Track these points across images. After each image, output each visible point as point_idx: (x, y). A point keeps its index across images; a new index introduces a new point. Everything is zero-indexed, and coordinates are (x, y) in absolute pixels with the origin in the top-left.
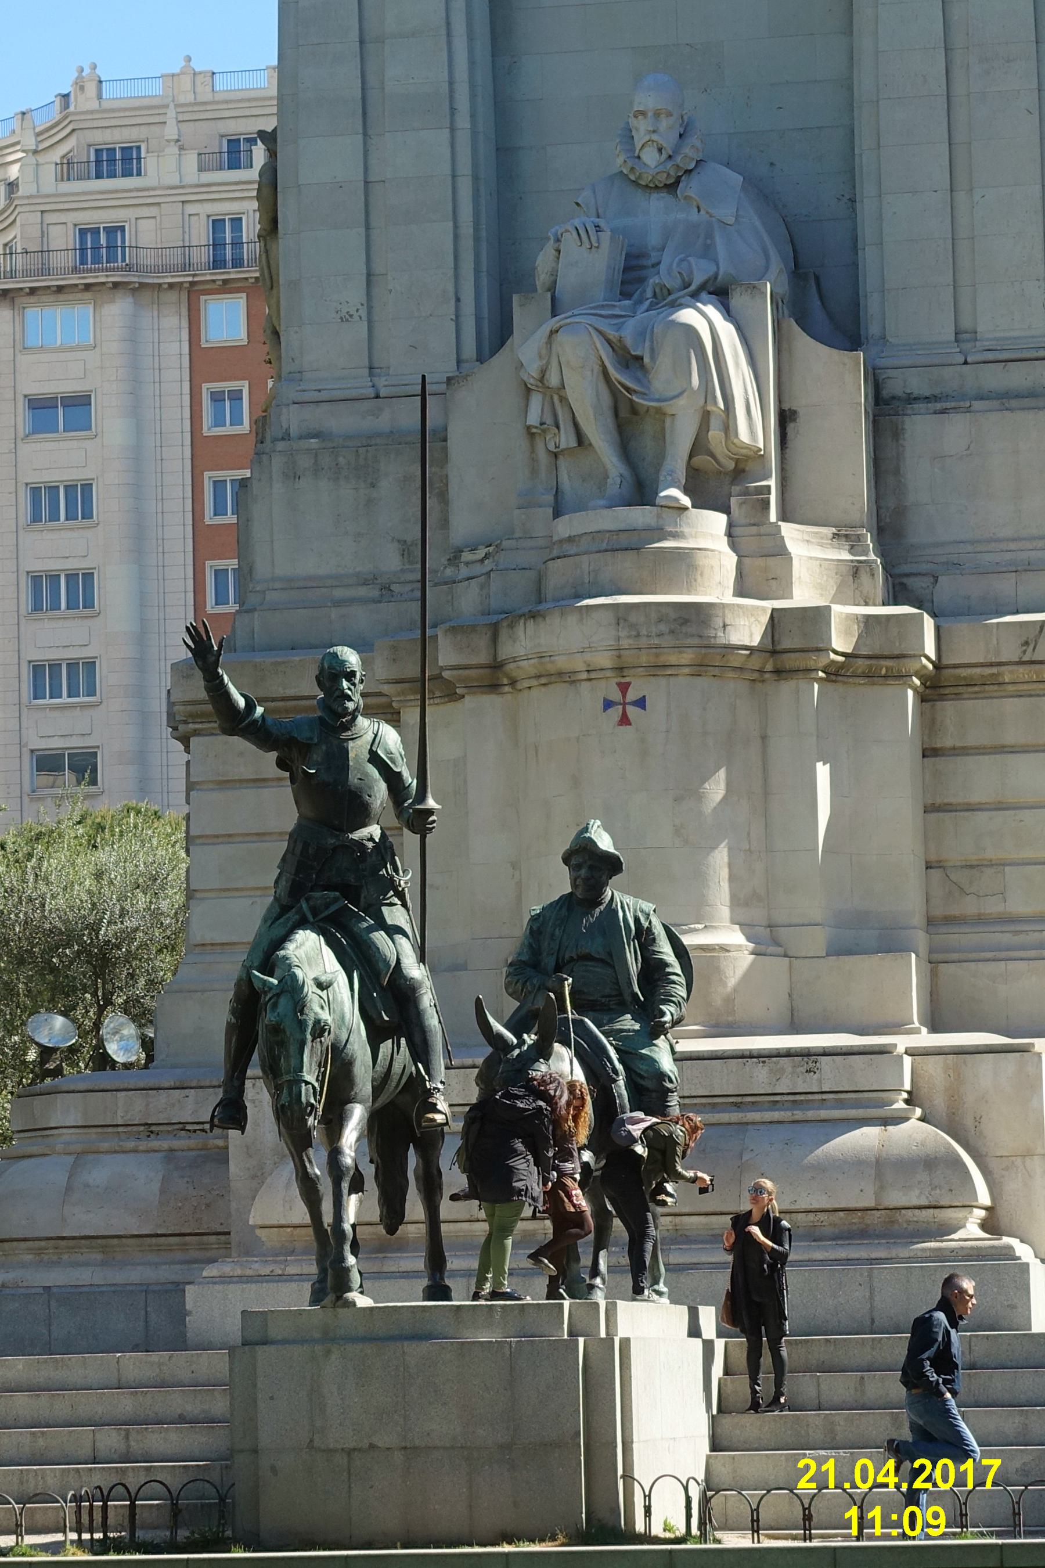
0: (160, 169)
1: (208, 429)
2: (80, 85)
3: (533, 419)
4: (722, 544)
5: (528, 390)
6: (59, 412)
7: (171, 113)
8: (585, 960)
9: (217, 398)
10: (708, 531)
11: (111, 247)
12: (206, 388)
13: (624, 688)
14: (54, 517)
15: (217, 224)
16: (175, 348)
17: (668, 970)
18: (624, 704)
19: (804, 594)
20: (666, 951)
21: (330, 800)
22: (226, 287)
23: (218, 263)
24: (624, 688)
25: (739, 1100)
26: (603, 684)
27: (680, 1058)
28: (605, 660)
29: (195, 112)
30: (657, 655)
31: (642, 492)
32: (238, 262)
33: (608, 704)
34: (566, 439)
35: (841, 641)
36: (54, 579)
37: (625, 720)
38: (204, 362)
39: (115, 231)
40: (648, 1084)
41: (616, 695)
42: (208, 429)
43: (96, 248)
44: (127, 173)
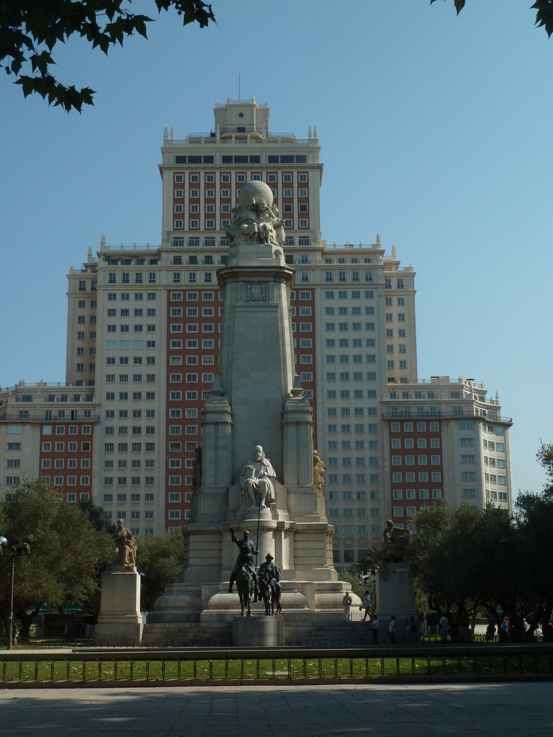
0: (38, 400)
1: (43, 451)
2: (20, 384)
3: (243, 493)
4: (270, 512)
5: (242, 490)
6: (15, 446)
7: (39, 390)
8: (269, 572)
9: (45, 445)
10: (268, 510)
11: (26, 416)
12: (43, 443)
14: (12, 466)
15: (47, 412)
16: (38, 435)
19: (280, 519)
21: (244, 550)
22: (48, 424)
23: (47, 419)
27: (281, 583)
29: (42, 391)
31: (259, 504)
32: (50, 419)
34: (247, 496)
35: (287, 526)
36: (11, 478)
38: (43, 438)
39: (27, 412)
42: (43, 451)
43: (23, 415)
44: (29, 401)
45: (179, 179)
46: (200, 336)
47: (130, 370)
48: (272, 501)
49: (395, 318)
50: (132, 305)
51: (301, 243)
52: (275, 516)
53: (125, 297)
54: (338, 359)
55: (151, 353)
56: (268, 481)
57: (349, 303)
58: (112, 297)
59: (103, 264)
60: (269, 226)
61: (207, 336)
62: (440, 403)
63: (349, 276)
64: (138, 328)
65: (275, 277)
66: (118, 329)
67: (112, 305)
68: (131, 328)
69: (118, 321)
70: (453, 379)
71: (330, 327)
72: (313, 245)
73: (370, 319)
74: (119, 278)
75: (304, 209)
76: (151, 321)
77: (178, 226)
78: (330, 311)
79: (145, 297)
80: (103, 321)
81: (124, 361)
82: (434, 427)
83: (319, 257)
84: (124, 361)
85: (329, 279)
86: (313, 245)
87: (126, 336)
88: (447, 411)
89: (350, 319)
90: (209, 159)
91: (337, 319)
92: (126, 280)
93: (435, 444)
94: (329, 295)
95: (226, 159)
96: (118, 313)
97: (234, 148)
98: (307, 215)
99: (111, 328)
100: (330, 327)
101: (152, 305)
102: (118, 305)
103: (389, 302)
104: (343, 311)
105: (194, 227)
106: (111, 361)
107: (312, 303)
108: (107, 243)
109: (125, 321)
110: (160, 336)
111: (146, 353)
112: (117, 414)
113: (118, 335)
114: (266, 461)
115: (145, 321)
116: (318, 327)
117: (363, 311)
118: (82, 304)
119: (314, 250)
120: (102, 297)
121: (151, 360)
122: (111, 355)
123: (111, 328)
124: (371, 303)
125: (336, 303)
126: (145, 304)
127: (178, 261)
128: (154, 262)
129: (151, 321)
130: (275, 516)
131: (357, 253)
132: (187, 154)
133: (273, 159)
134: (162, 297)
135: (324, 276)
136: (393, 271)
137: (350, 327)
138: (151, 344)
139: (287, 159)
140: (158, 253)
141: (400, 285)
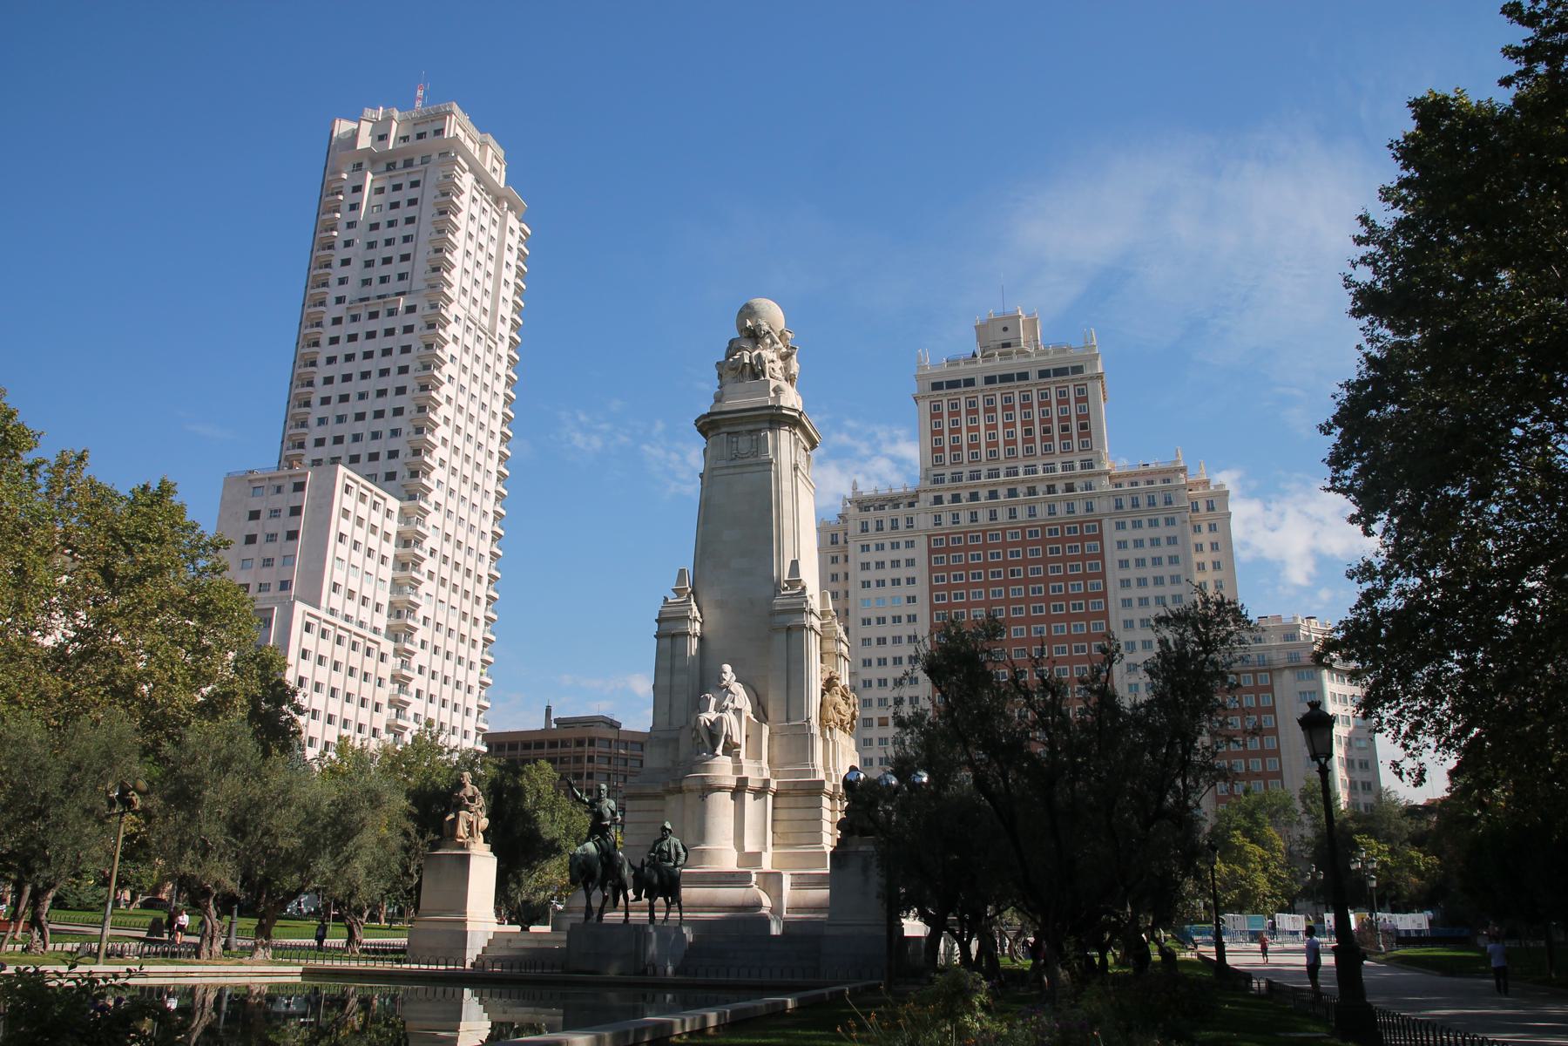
10: (727, 761)
45: (937, 408)
46: (968, 586)
47: (888, 631)
48: (738, 746)
49: (1207, 547)
50: (888, 555)
51: (1083, 467)
52: (738, 768)
53: (880, 547)
54: (1135, 603)
55: (912, 609)
56: (729, 717)
57: (1146, 533)
58: (865, 548)
59: (853, 511)
60: (768, 354)
61: (976, 585)
62: (1269, 648)
63: (1143, 501)
64: (896, 582)
65: (771, 422)
66: (873, 584)
67: (865, 557)
68: (888, 583)
69: (873, 575)
70: (1287, 618)
71: (1124, 564)
72: (1097, 468)
73: (1172, 550)
74: (872, 526)
75: (1084, 426)
76: (911, 572)
77: (938, 460)
78: (1122, 545)
79: (902, 545)
80: (858, 576)
81: (881, 620)
82: (1264, 679)
83: (1106, 481)
84: (881, 620)
85: (1119, 506)
86: (1097, 468)
87: (881, 591)
88: (1279, 658)
89: (1147, 552)
90: (970, 382)
91: (1131, 554)
92: (880, 527)
93: (1265, 700)
94: (1120, 526)
95: (990, 380)
96: (873, 565)
97: (998, 366)
98: (1089, 435)
99: (866, 584)
100: (1124, 564)
101: (910, 553)
102: (873, 557)
103: (1197, 529)
104: (1139, 543)
105: (956, 460)
106: (867, 622)
107: (1100, 537)
108: (860, 489)
109: (880, 574)
110: (921, 590)
111: (905, 610)
112: (875, 683)
113: (874, 591)
114: (737, 688)
115: (903, 573)
116: (1108, 565)
117: (1163, 541)
118: (834, 560)
119: (1100, 474)
120: (853, 548)
121: (912, 619)
122: (866, 616)
123: (866, 584)
124: (1171, 531)
125: (1129, 535)
126: (903, 554)
127: (938, 500)
128: (911, 505)
129: (911, 572)
130: (738, 768)
131: (1152, 473)
132: (944, 379)
133: (1044, 374)
134: (922, 544)
135: (1113, 503)
136: (1201, 491)
137: (1149, 562)
138: (911, 599)
139: (1060, 372)
140: (916, 495)
141: (1210, 507)
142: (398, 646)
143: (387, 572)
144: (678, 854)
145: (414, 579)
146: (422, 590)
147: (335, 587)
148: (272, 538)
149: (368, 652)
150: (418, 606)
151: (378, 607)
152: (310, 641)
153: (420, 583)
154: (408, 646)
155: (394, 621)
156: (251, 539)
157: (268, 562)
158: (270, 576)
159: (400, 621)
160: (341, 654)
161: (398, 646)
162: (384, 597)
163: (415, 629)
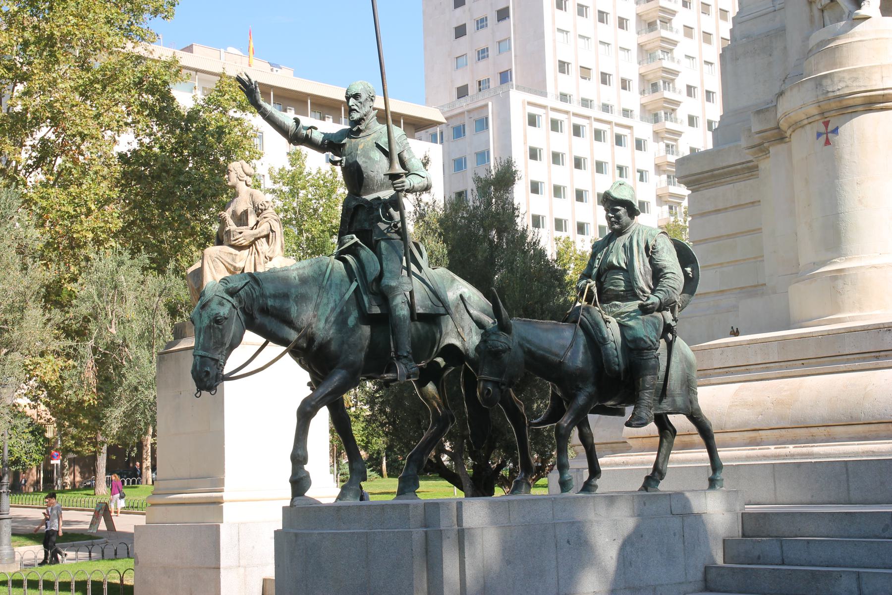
13: (826, 124)
17: (666, 271)
18: (827, 133)
20: (669, 259)
24: (826, 124)
25: (877, 354)
26: (815, 124)
28: (813, 110)
30: (840, 101)
33: (819, 135)
37: (827, 142)
40: (631, 346)
41: (822, 129)
142: (658, 127)
143: (631, 38)
144: (658, 274)
145: (664, 40)
146: (678, 52)
147: (563, 67)
148: (482, 23)
149: (619, 140)
150: (676, 73)
151: (625, 84)
152: (540, 137)
153: (674, 43)
154: (669, 125)
155: (648, 98)
156: (460, 31)
157: (483, 54)
158: (487, 70)
159: (657, 96)
160: (583, 147)
161: (658, 127)
162: (632, 69)
163: (678, 103)
